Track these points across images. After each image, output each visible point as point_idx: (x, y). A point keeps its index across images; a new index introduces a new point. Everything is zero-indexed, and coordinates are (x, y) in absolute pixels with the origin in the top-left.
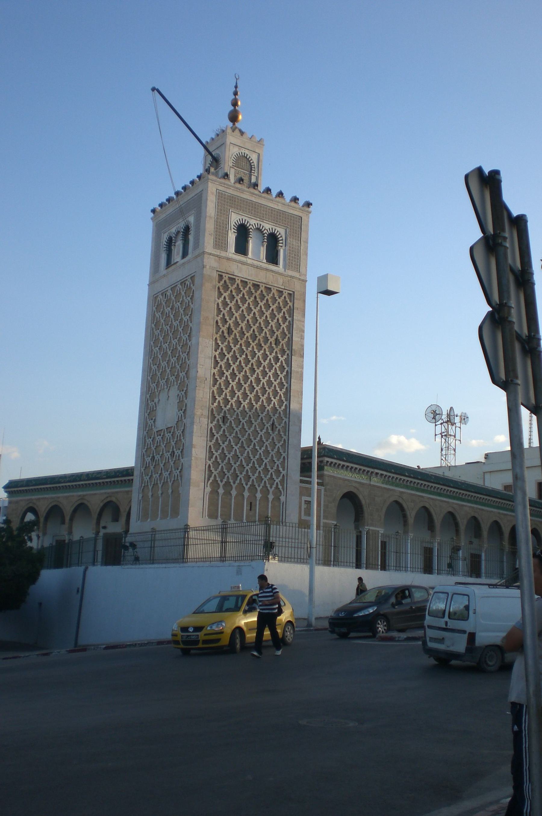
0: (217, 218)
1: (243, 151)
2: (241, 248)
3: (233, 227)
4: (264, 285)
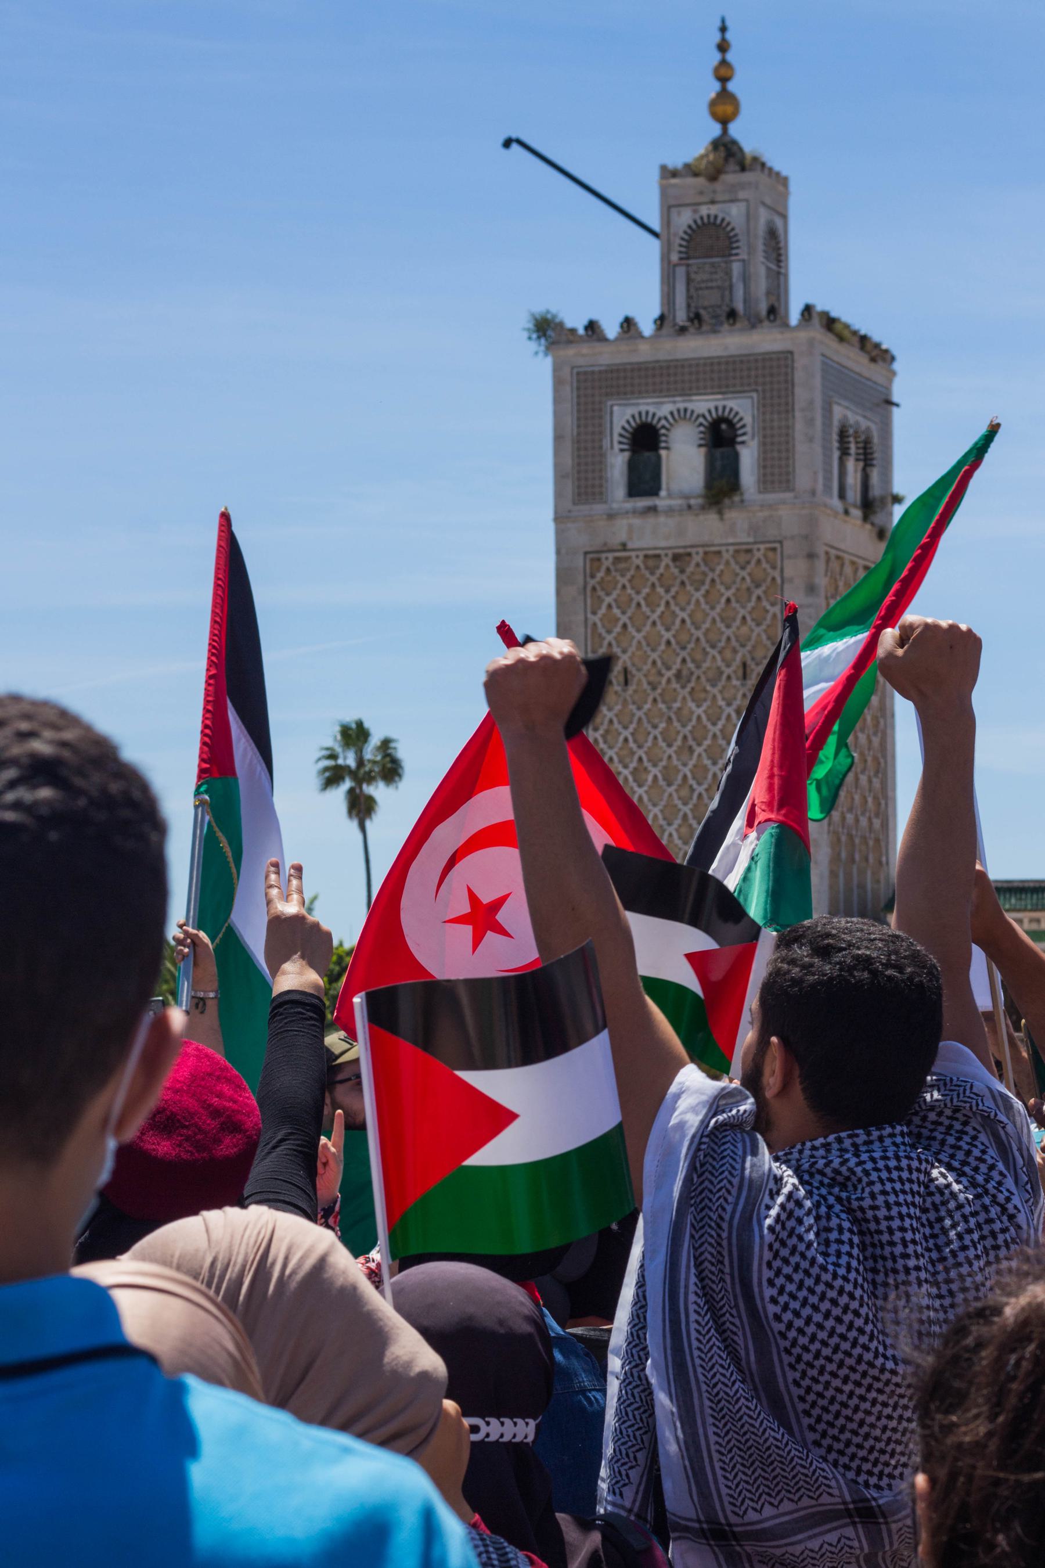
0: (579, 434)
1: (704, 210)
2: (644, 480)
3: (616, 438)
4: (701, 550)
